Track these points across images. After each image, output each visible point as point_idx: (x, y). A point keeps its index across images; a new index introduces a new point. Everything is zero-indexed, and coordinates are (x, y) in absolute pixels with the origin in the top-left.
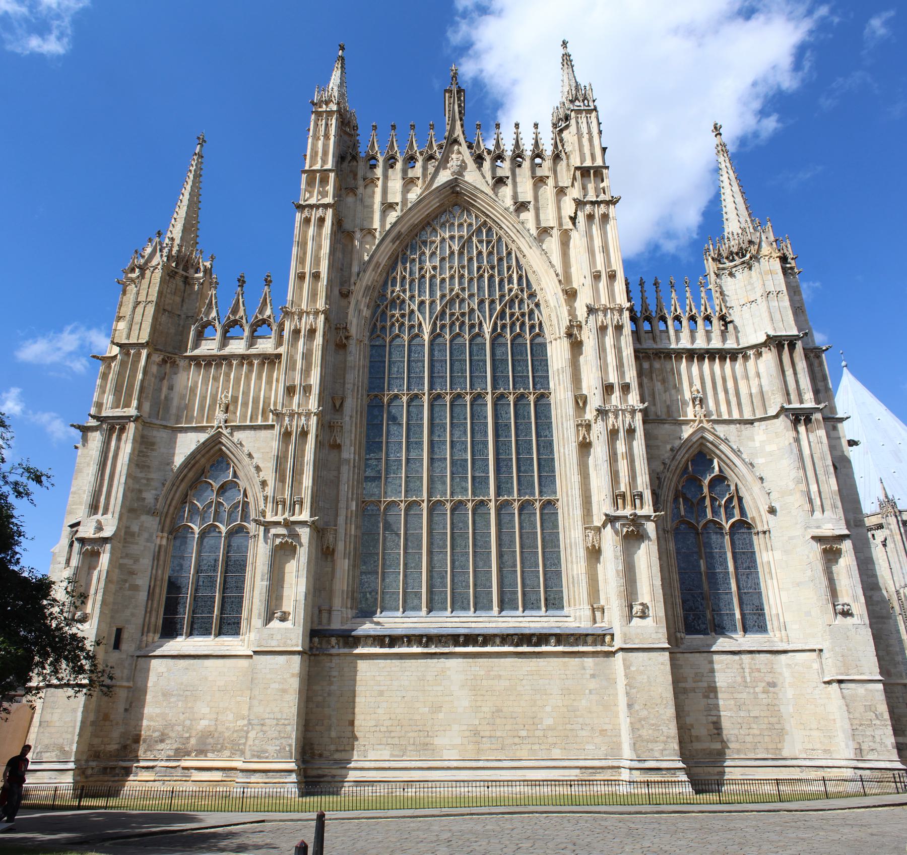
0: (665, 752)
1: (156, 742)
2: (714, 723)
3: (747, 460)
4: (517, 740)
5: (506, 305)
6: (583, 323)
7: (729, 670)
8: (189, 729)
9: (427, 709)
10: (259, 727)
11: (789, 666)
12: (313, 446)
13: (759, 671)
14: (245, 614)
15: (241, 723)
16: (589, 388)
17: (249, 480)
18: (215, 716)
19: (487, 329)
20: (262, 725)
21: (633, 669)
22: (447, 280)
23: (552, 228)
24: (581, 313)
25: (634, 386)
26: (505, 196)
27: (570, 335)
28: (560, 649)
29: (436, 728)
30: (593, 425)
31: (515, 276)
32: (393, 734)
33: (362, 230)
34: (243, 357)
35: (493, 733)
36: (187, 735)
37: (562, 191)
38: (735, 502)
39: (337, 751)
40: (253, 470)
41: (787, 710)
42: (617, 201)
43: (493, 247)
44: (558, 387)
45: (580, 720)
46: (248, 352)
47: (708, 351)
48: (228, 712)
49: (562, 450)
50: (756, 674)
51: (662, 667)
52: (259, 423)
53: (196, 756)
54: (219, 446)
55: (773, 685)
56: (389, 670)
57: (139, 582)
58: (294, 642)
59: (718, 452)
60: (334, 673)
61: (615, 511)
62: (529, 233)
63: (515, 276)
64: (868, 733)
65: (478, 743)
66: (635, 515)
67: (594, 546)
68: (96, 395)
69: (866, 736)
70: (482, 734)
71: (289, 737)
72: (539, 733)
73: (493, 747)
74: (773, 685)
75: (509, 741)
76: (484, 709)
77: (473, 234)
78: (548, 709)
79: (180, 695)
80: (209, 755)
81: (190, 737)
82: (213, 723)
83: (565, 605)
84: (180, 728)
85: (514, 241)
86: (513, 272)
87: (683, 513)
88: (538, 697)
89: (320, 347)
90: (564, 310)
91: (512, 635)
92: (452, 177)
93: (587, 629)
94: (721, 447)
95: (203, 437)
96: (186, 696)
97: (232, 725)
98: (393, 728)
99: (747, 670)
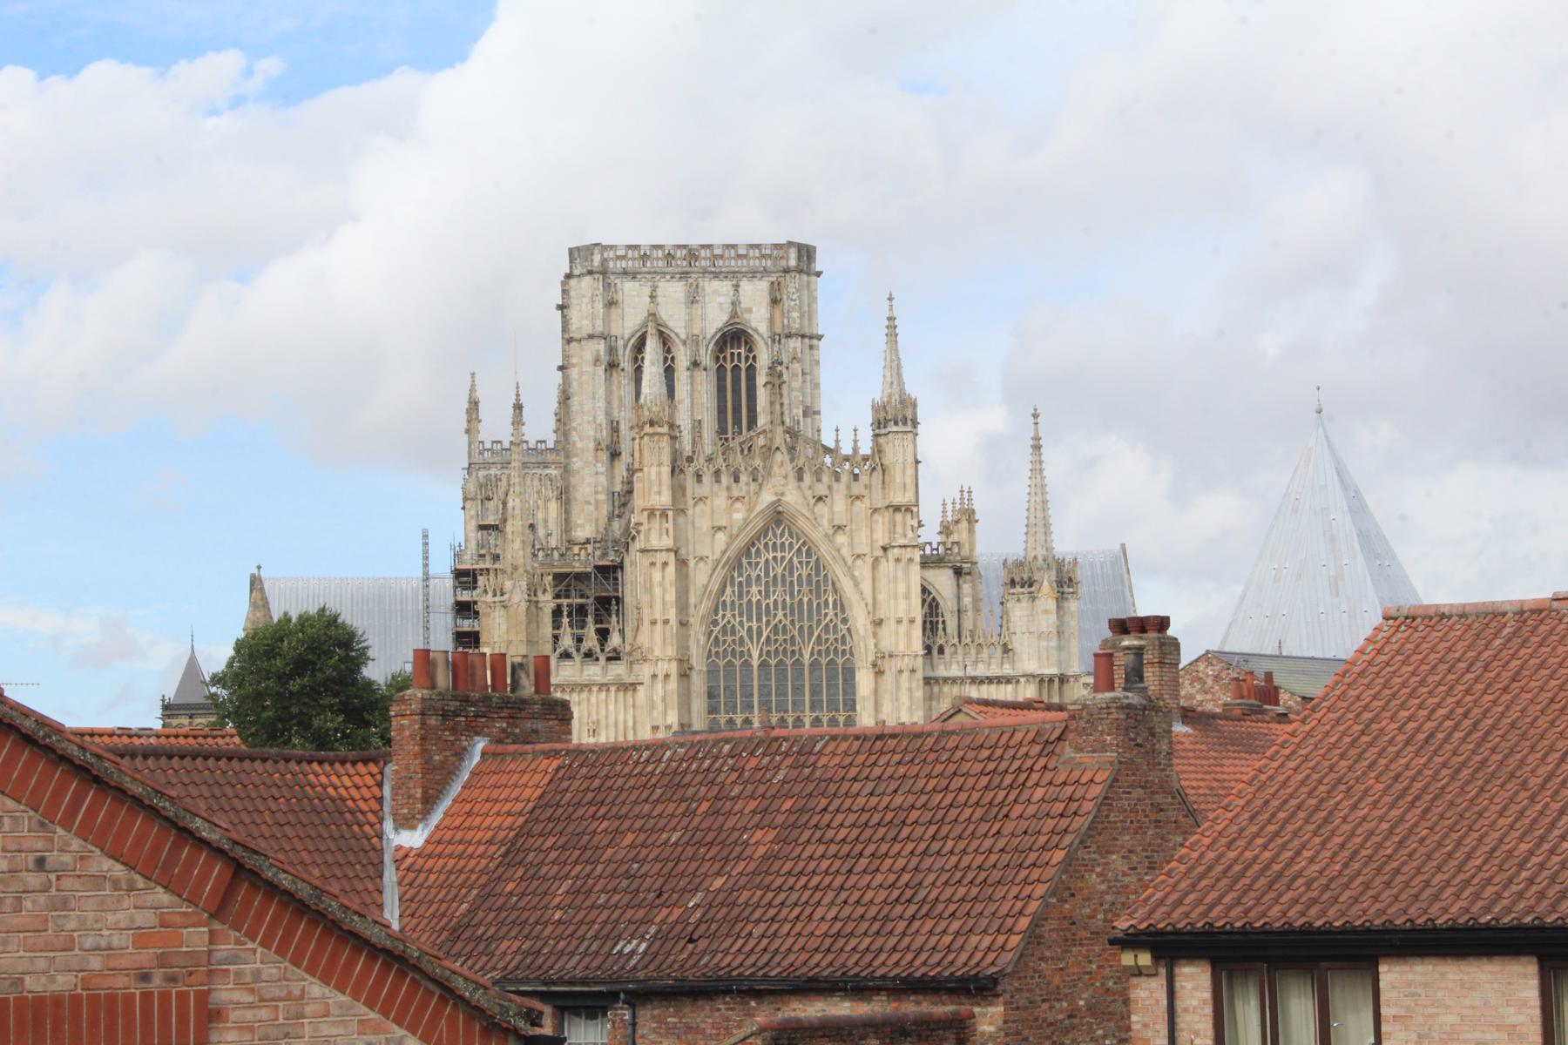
27: (874, 665)
31: (831, 600)
34: (602, 685)
47: (987, 678)
63: (831, 600)
90: (871, 642)
92: (774, 498)
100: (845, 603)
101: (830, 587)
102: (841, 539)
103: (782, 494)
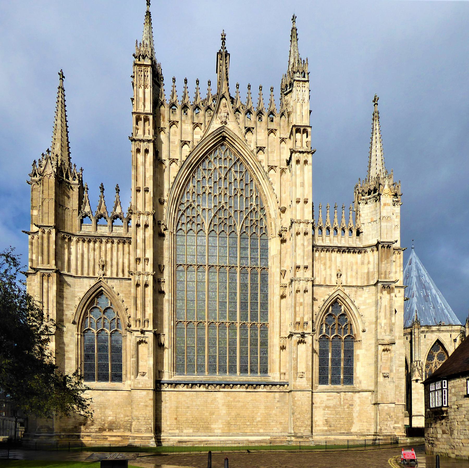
0: (305, 431)
1: (90, 425)
2: (326, 420)
3: (357, 307)
4: (245, 426)
6: (288, 229)
7: (335, 399)
8: (104, 420)
9: (208, 414)
10: (137, 420)
11: (359, 398)
13: (347, 400)
14: (124, 372)
15: (127, 418)
16: (288, 267)
17: (118, 307)
18: (115, 415)
19: (238, 228)
20: (138, 419)
21: (296, 399)
23: (276, 167)
24: (287, 224)
25: (310, 267)
27: (280, 235)
28: (265, 390)
29: (212, 421)
32: (193, 423)
35: (236, 423)
36: (104, 423)
38: (348, 327)
39: (170, 429)
40: (121, 302)
41: (355, 415)
42: (313, 153)
43: (243, 176)
44: (272, 265)
45: (272, 419)
46: (111, 235)
48: (121, 414)
50: (346, 401)
51: (308, 398)
52: (120, 276)
53: (108, 431)
54: (102, 288)
55: (352, 405)
56: (191, 398)
57: (71, 356)
58: (149, 386)
59: (344, 302)
60: (167, 399)
62: (264, 170)
64: (385, 423)
65: (229, 427)
66: (304, 333)
67: (283, 346)
68: (30, 254)
69: (384, 424)
70: (231, 423)
71: (151, 424)
72: (255, 423)
73: (236, 428)
74: (352, 405)
75: (242, 426)
76: (232, 414)
77: (232, 167)
78: (259, 414)
79: (98, 406)
80: (114, 430)
81: (105, 423)
82: (114, 418)
84: (100, 420)
85: (255, 173)
87: (324, 331)
88: (255, 409)
91: (245, 384)
93: (277, 382)
94: (346, 300)
95: (93, 282)
96: (101, 407)
97: (123, 419)
98: (194, 421)
99: (342, 400)
102: (261, 156)
103: (226, 123)
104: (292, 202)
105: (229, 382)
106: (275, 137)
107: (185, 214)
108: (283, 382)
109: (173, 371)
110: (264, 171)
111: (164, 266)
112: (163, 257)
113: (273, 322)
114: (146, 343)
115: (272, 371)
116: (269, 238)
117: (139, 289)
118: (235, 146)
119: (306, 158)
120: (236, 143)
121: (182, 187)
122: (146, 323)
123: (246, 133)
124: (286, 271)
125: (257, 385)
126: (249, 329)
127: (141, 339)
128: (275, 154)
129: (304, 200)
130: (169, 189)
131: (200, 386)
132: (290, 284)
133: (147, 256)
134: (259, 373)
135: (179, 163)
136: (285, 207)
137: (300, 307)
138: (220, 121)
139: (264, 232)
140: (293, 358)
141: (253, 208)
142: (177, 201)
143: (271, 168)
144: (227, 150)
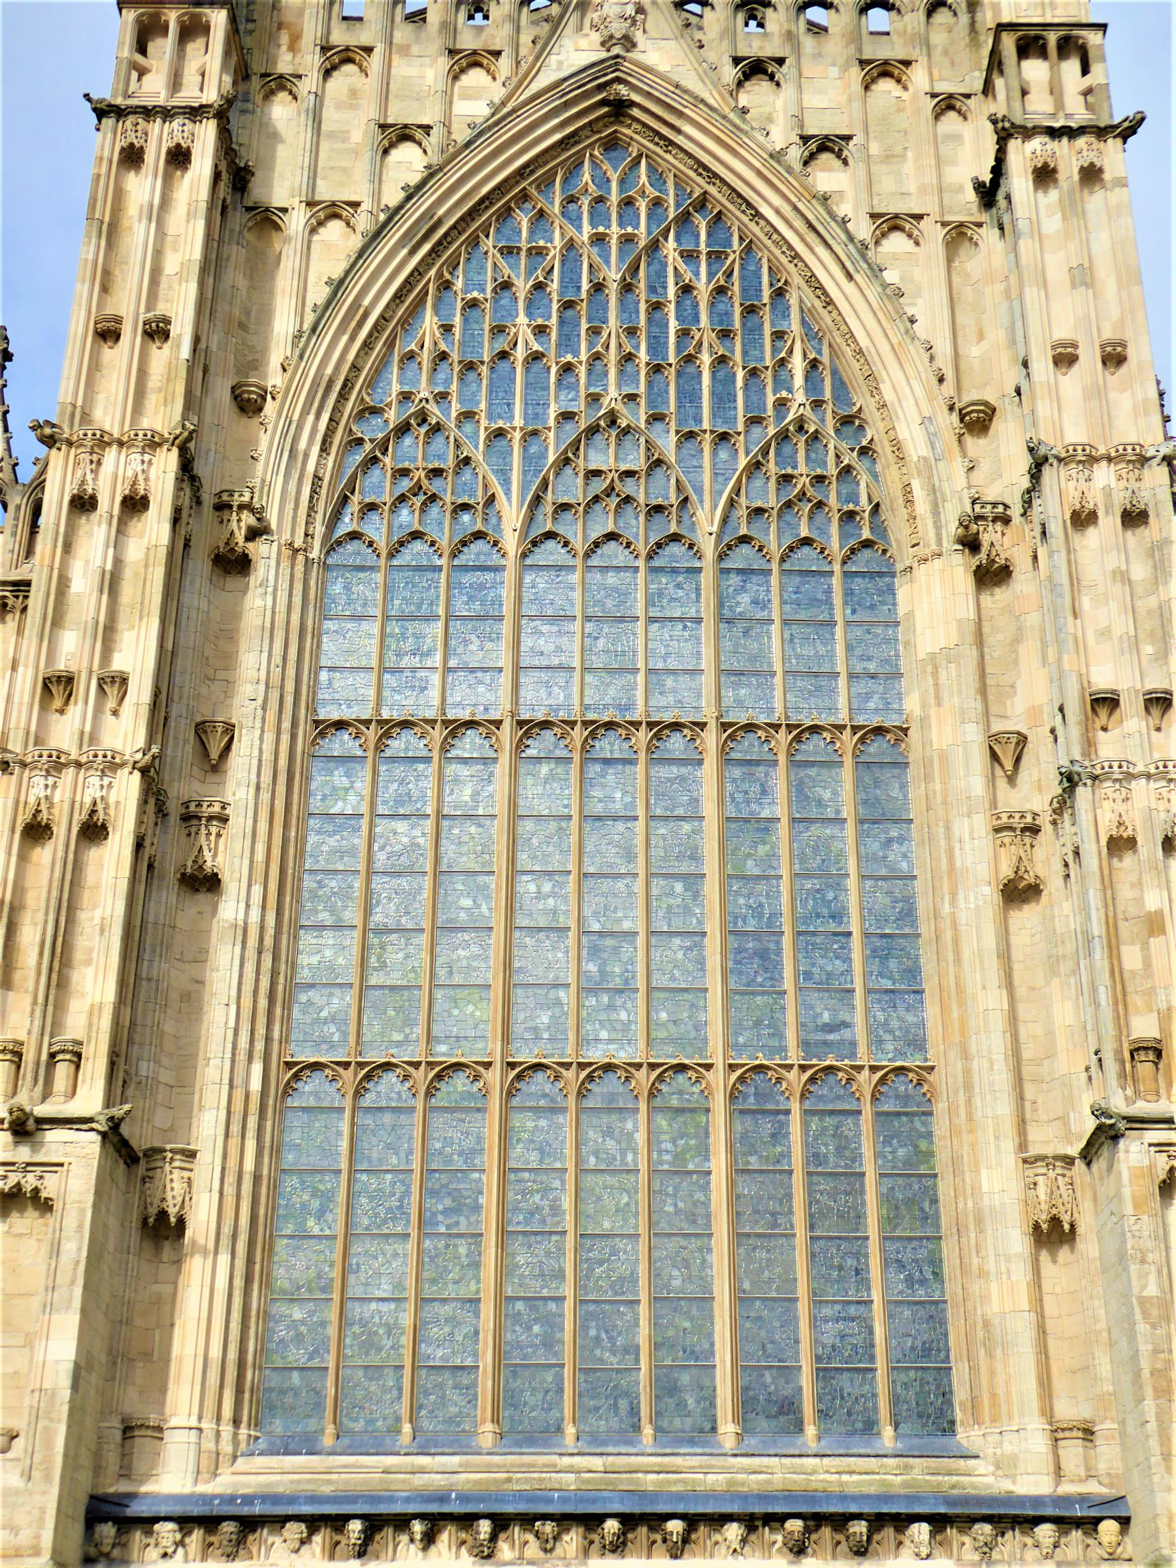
5: (765, 452)
6: (1015, 512)
12: (125, 872)
22: (582, 370)
23: (919, 217)
26: (770, 119)
27: (971, 544)
30: (1047, 828)
31: (798, 365)
33: (310, 204)
37: (951, 107)
43: (729, 274)
44: (933, 711)
49: (946, 909)
61: (1129, 1101)
62: (847, 232)
63: (798, 365)
67: (1055, 1221)
83: (959, 1415)
86: (791, 351)
89: (162, 553)
91: (782, 1518)
92: (604, 55)
100: (853, 369)
101: (794, 326)
103: (628, 42)
104: (1025, 364)
105: (655, 1496)
106: (905, 96)
107: (387, 460)
108: (1083, 1499)
109: (236, 1422)
110: (851, 239)
111: (230, 729)
112: (229, 684)
113: (966, 1055)
114: (44, 1206)
115: (986, 1414)
116: (899, 567)
117: (45, 855)
118: (679, 140)
119: (1089, 157)
120: (688, 128)
121: (377, 328)
122: (62, 1070)
123: (740, 84)
124: (1022, 740)
125: (878, 1521)
126: (795, 1106)
127: (13, 1179)
128: (909, 167)
129: (1102, 347)
130: (298, 336)
131: (429, 1539)
132: (1058, 811)
133: (119, 663)
134: (888, 1432)
135: (364, 222)
136: (986, 404)
137: (1145, 947)
138: (596, 37)
139: (866, 534)
140: (1143, 1301)
141: (790, 417)
142: (343, 396)
143: (890, 224)
144: (636, 162)
